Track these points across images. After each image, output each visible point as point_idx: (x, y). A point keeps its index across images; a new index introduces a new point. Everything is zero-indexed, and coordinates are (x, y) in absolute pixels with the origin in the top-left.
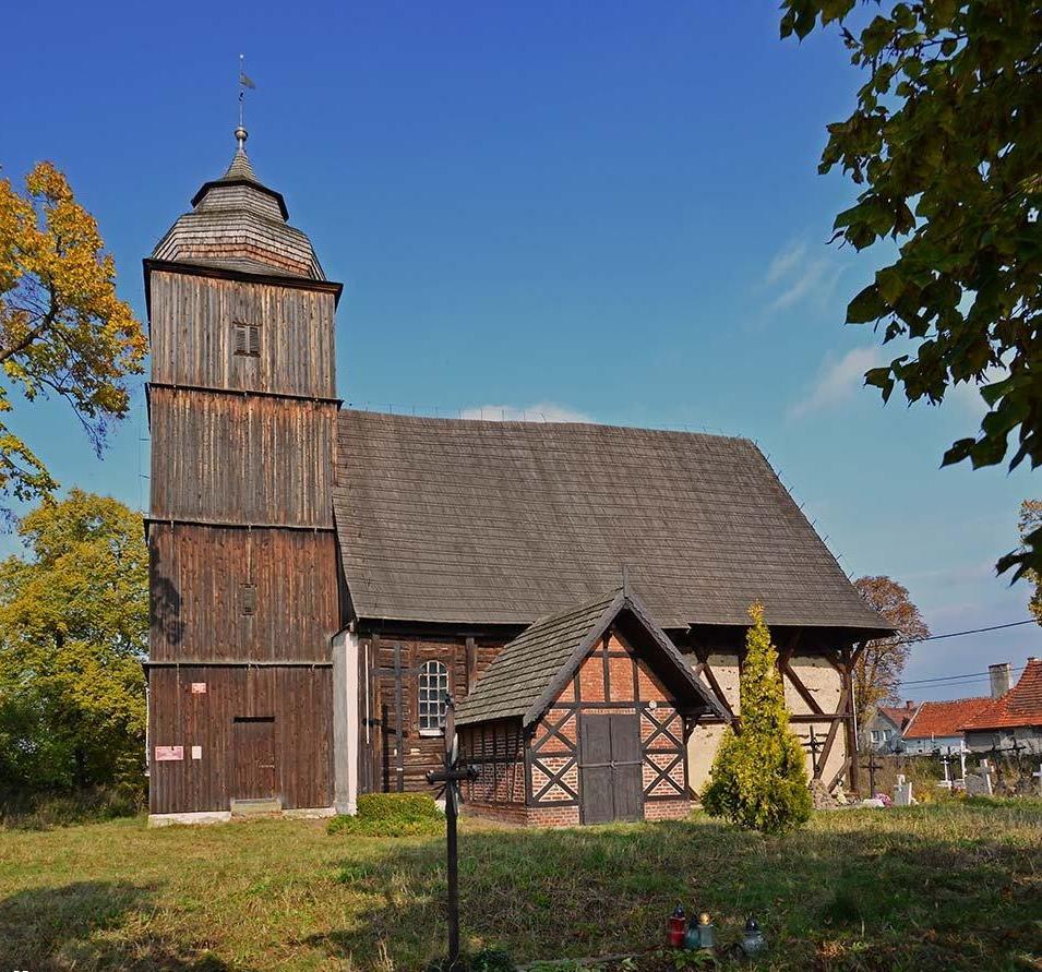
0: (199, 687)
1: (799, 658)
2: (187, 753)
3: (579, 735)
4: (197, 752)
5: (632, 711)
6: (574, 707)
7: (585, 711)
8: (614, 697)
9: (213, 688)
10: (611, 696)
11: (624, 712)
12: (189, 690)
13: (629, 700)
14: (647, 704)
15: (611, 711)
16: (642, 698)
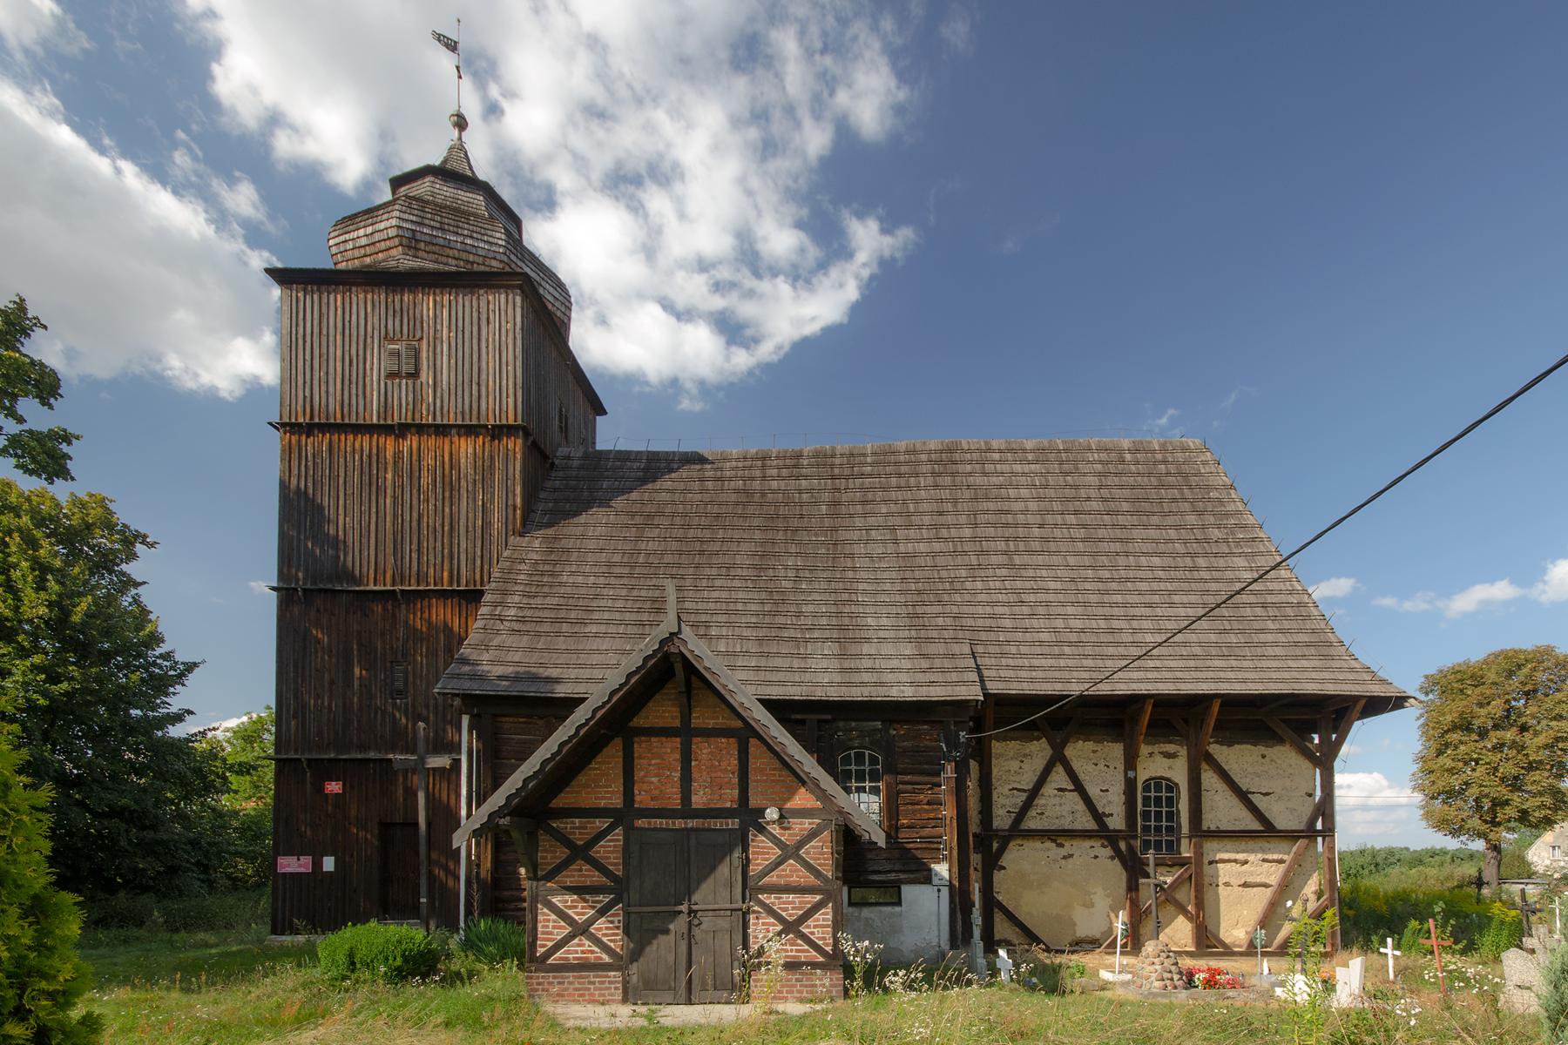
0: (334, 787)
1: (1237, 747)
2: (317, 864)
3: (626, 863)
4: (329, 864)
5: (733, 823)
6: (624, 815)
7: (640, 823)
8: (699, 800)
9: (352, 787)
10: (694, 799)
11: (717, 824)
12: (320, 790)
13: (728, 805)
14: (761, 812)
15: (691, 823)
16: (754, 802)
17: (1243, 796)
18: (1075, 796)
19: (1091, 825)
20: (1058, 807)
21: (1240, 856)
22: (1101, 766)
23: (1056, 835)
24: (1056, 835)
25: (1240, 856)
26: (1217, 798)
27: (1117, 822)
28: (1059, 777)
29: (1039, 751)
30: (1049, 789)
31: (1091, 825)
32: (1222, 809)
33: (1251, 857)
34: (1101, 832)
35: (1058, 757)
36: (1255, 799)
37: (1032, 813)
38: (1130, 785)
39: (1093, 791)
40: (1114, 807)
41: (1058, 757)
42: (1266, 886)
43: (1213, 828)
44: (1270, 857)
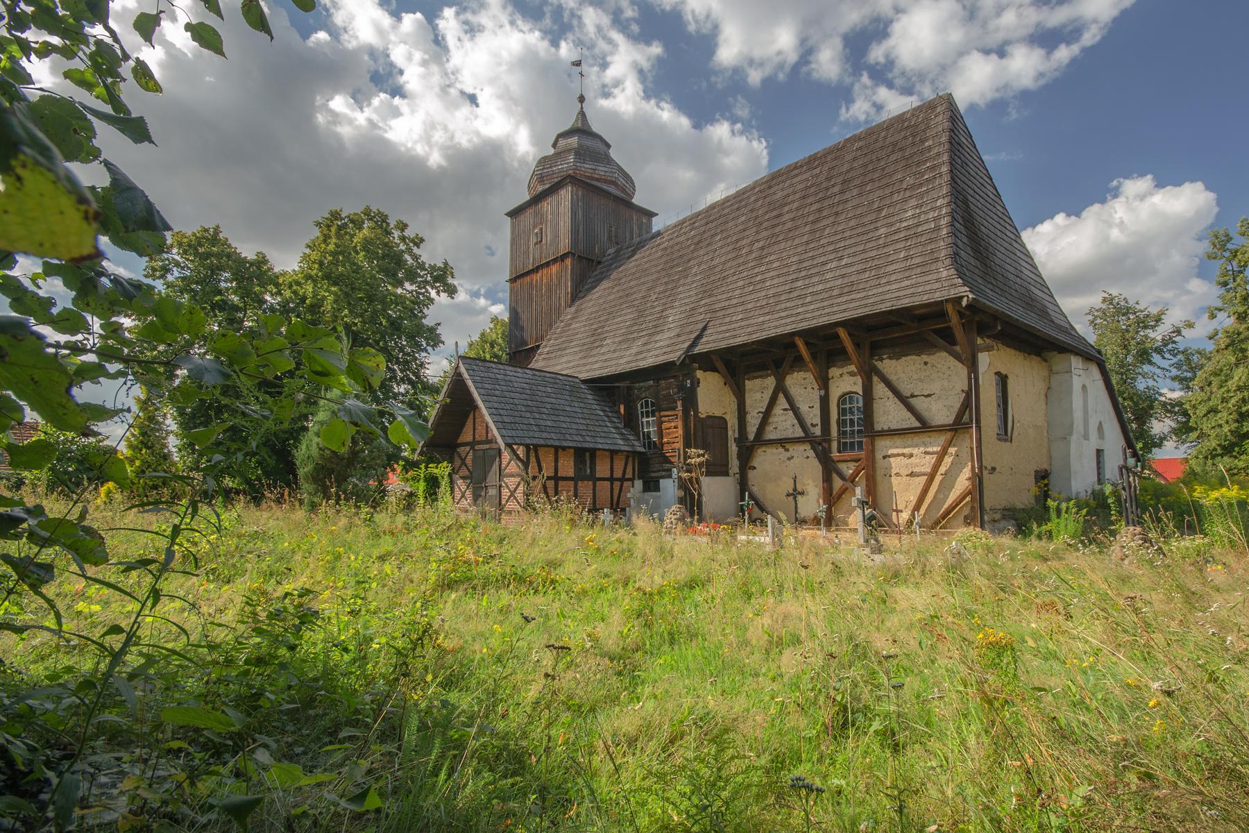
17: (904, 400)
18: (791, 413)
19: (799, 433)
20: (783, 424)
21: (906, 451)
22: (809, 389)
23: (783, 442)
24: (783, 442)
25: (906, 451)
26: (888, 404)
27: (817, 431)
28: (782, 402)
29: (771, 382)
30: (778, 410)
31: (799, 433)
32: (889, 413)
33: (915, 451)
34: (807, 438)
35: (780, 388)
36: (918, 403)
37: (769, 428)
38: (825, 401)
39: (804, 408)
40: (813, 416)
41: (780, 388)
42: (924, 474)
43: (886, 428)
44: (930, 449)
